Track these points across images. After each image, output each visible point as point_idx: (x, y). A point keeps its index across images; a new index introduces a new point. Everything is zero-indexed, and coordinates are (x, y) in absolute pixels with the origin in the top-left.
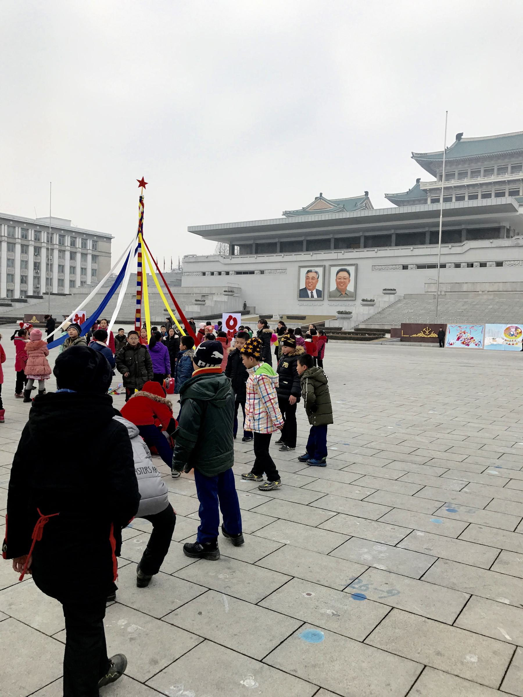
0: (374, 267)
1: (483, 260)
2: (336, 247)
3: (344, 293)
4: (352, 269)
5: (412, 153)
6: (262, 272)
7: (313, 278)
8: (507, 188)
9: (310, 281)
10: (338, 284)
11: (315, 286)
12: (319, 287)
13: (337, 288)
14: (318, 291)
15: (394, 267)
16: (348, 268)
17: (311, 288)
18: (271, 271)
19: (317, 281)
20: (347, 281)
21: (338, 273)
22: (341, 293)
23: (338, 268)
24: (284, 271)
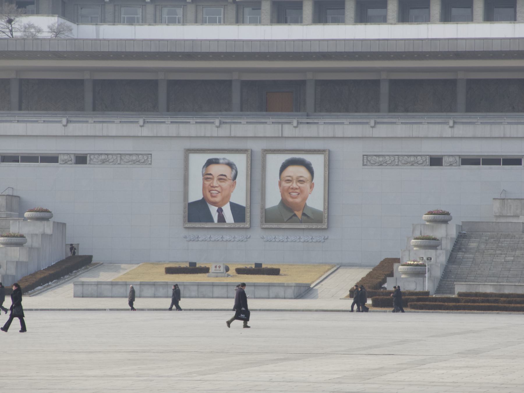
0: (368, 160)
2: (472, 107)
3: (299, 214)
4: (317, 162)
6: (81, 159)
7: (222, 178)
9: (215, 183)
10: (284, 191)
11: (228, 196)
12: (239, 196)
13: (284, 203)
15: (411, 161)
17: (218, 199)
18: (105, 159)
19: (233, 185)
20: (307, 185)
21: (284, 167)
22: (290, 214)
24: (144, 159)
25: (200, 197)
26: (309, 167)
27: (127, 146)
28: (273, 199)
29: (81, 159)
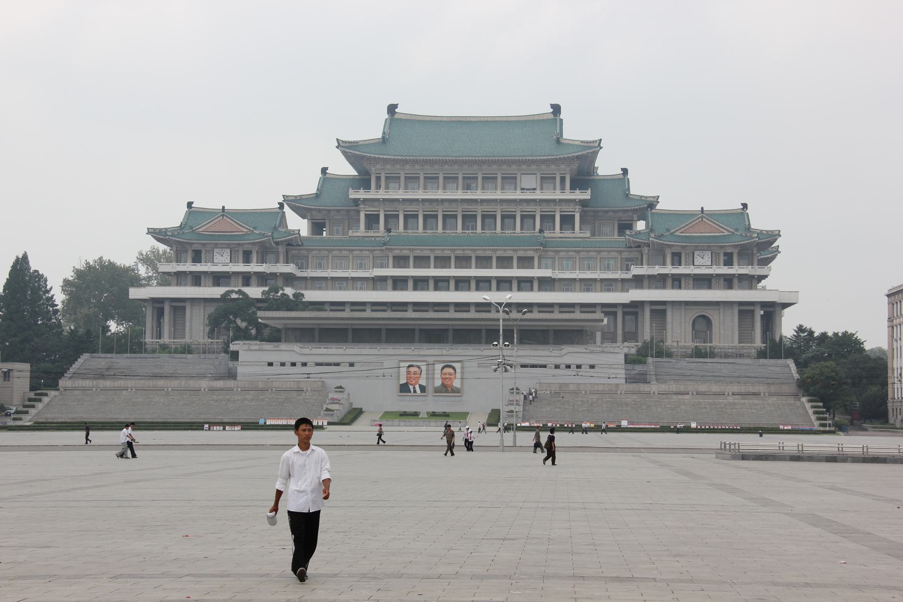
1: (579, 363)
4: (457, 366)
5: (337, 140)
7: (415, 373)
8: (479, 210)
12: (423, 382)
13: (443, 384)
14: (420, 386)
16: (454, 364)
20: (453, 377)
21: (443, 368)
22: (445, 389)
23: (443, 365)
25: (405, 381)
26: (454, 368)
27: (372, 359)
28: (438, 383)
29: (352, 365)
